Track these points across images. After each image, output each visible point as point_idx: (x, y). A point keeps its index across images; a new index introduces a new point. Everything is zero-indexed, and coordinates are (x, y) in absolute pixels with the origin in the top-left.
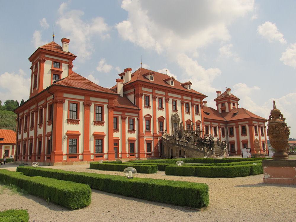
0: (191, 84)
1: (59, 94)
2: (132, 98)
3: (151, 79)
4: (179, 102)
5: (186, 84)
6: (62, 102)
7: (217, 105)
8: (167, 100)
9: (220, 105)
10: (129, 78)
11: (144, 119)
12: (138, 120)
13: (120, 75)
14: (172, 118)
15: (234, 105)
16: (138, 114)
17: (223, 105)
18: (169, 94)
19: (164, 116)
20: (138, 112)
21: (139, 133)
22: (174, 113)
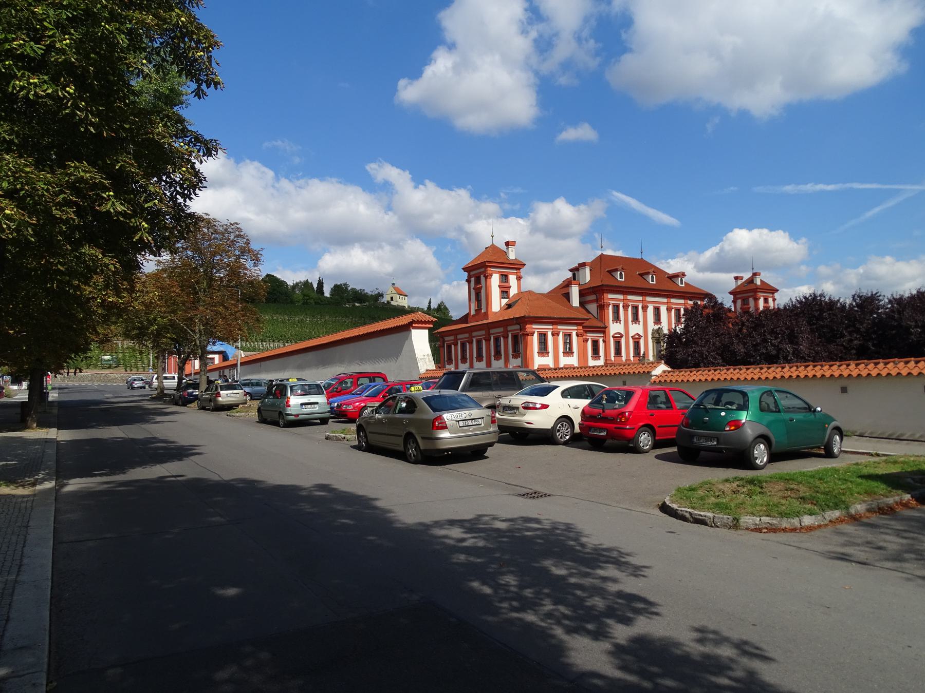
0: (684, 275)
1: (528, 326)
2: (593, 307)
3: (620, 277)
4: (663, 309)
5: (676, 276)
6: (533, 334)
7: (734, 302)
8: (645, 308)
9: (739, 302)
10: (586, 276)
11: (612, 339)
12: (604, 341)
13: (571, 270)
14: (653, 334)
15: (766, 300)
16: (604, 332)
17: (745, 301)
18: (648, 299)
19: (642, 334)
20: (603, 330)
21: (606, 360)
22: (657, 327)
